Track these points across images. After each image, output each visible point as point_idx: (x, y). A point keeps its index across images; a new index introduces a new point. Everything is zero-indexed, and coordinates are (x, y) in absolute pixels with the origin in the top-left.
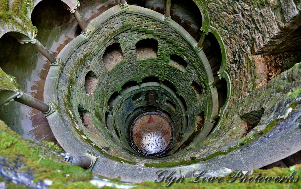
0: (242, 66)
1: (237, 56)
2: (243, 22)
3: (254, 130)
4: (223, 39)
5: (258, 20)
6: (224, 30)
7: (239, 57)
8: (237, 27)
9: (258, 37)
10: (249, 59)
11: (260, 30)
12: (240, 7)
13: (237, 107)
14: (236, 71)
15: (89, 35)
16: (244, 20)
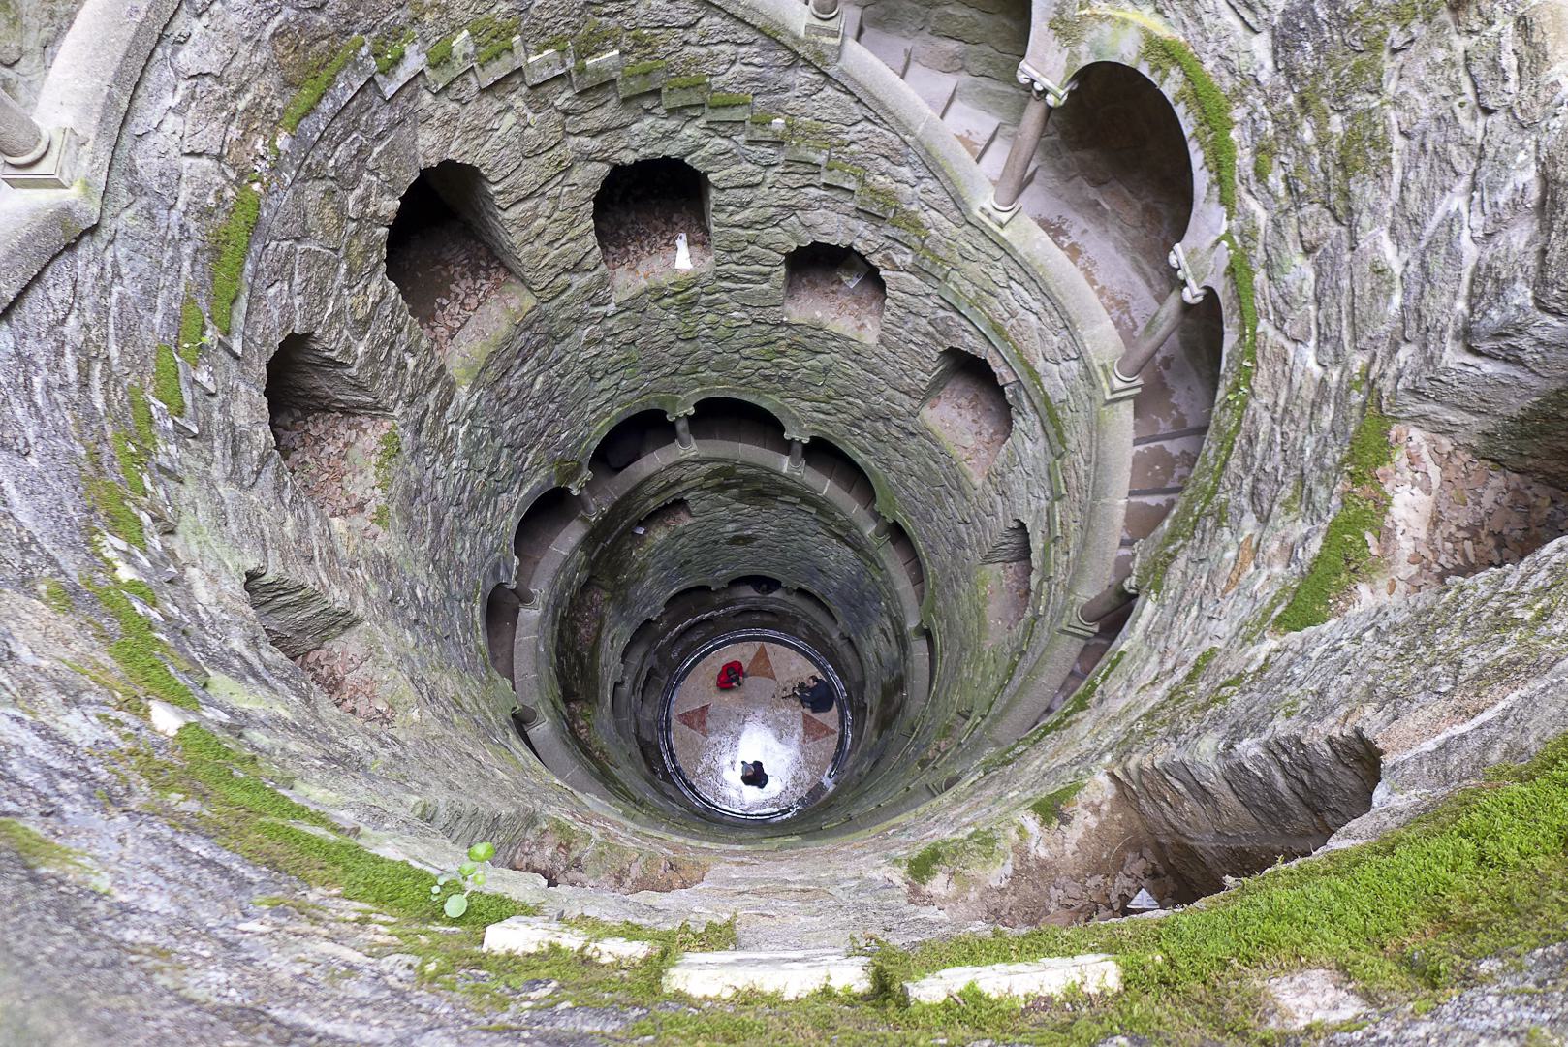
15: (986, 220)
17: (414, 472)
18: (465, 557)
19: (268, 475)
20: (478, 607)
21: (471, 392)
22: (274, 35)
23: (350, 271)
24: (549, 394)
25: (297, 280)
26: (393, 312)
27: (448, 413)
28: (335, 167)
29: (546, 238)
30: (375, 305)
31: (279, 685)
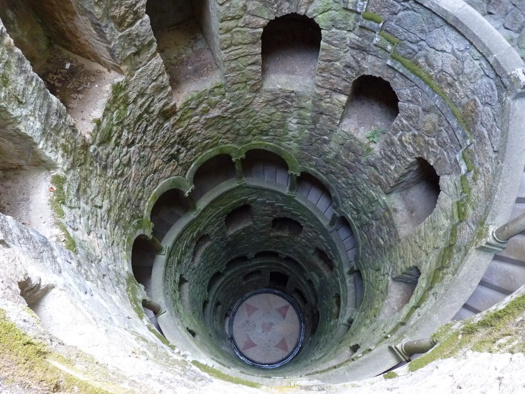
0: (186, 132)
1: (173, 151)
2: (140, 140)
3: (306, 11)
4: (154, 189)
5: (141, 106)
6: (146, 189)
7: (173, 145)
8: (144, 156)
9: (159, 101)
10: (182, 116)
11: (150, 99)
12: (125, 150)
13: (243, 110)
14: (188, 147)
16: (137, 141)
18: (340, 181)
22: (475, 100)
23: (414, 135)
25: (411, 105)
26: (404, 158)
27: (379, 187)
28: (442, 130)
30: (405, 147)
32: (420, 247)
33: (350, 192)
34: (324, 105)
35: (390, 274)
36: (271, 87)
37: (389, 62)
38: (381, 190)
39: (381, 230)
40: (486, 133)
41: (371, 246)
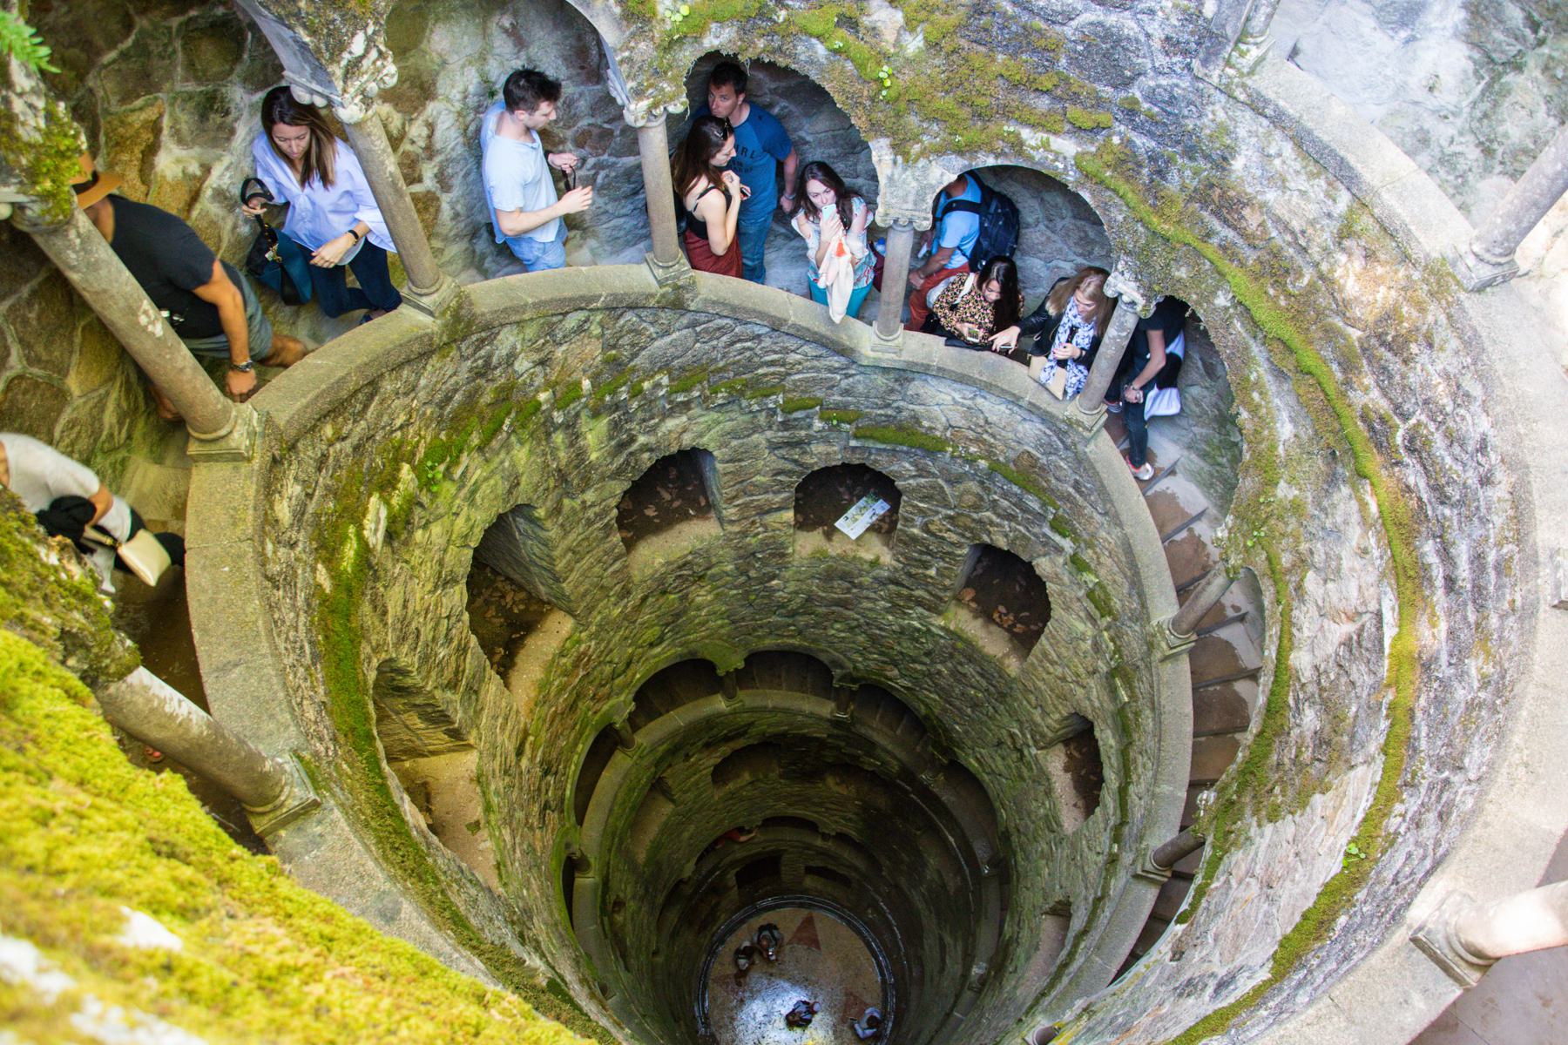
17: (867, 580)
19: (789, 466)
20: (796, 642)
21: (942, 628)
24: (975, 705)
27: (920, 610)
29: (1045, 675)
31: (621, 459)
32: (1063, 679)
33: (861, 638)
34: (753, 541)
35: (1031, 742)
36: (648, 572)
37: (853, 443)
38: (926, 613)
39: (965, 675)
40: (1071, 490)
41: (959, 709)
